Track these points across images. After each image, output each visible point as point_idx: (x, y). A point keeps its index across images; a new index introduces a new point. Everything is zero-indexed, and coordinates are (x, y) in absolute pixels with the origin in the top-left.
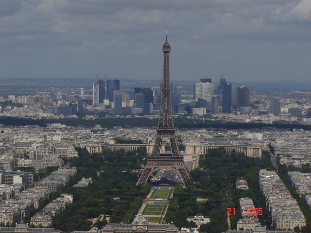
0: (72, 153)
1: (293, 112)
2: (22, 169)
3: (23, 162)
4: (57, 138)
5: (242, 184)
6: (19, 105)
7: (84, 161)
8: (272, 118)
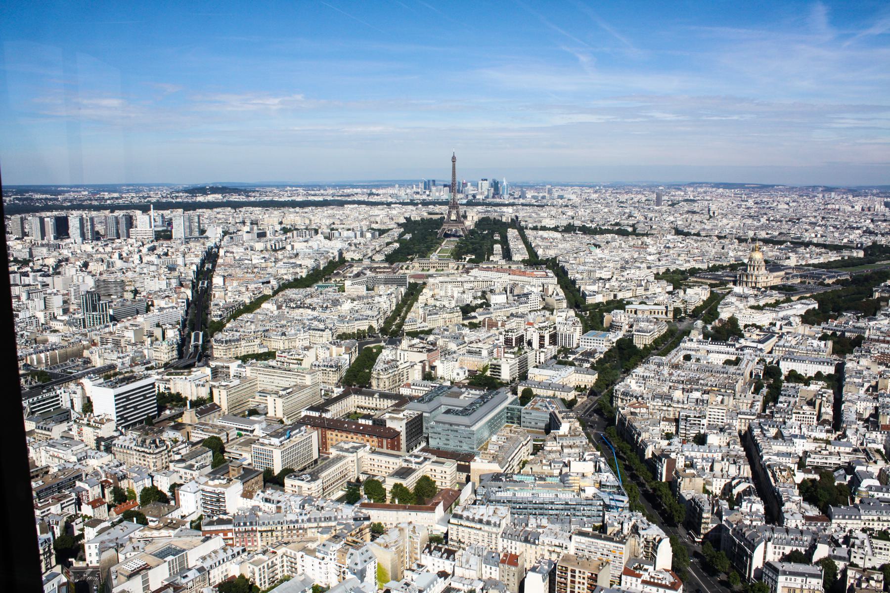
0: (403, 221)
1: (533, 197)
2: (372, 229)
3: (374, 226)
5: (497, 237)
6: (378, 195)
7: (408, 225)
8: (521, 201)
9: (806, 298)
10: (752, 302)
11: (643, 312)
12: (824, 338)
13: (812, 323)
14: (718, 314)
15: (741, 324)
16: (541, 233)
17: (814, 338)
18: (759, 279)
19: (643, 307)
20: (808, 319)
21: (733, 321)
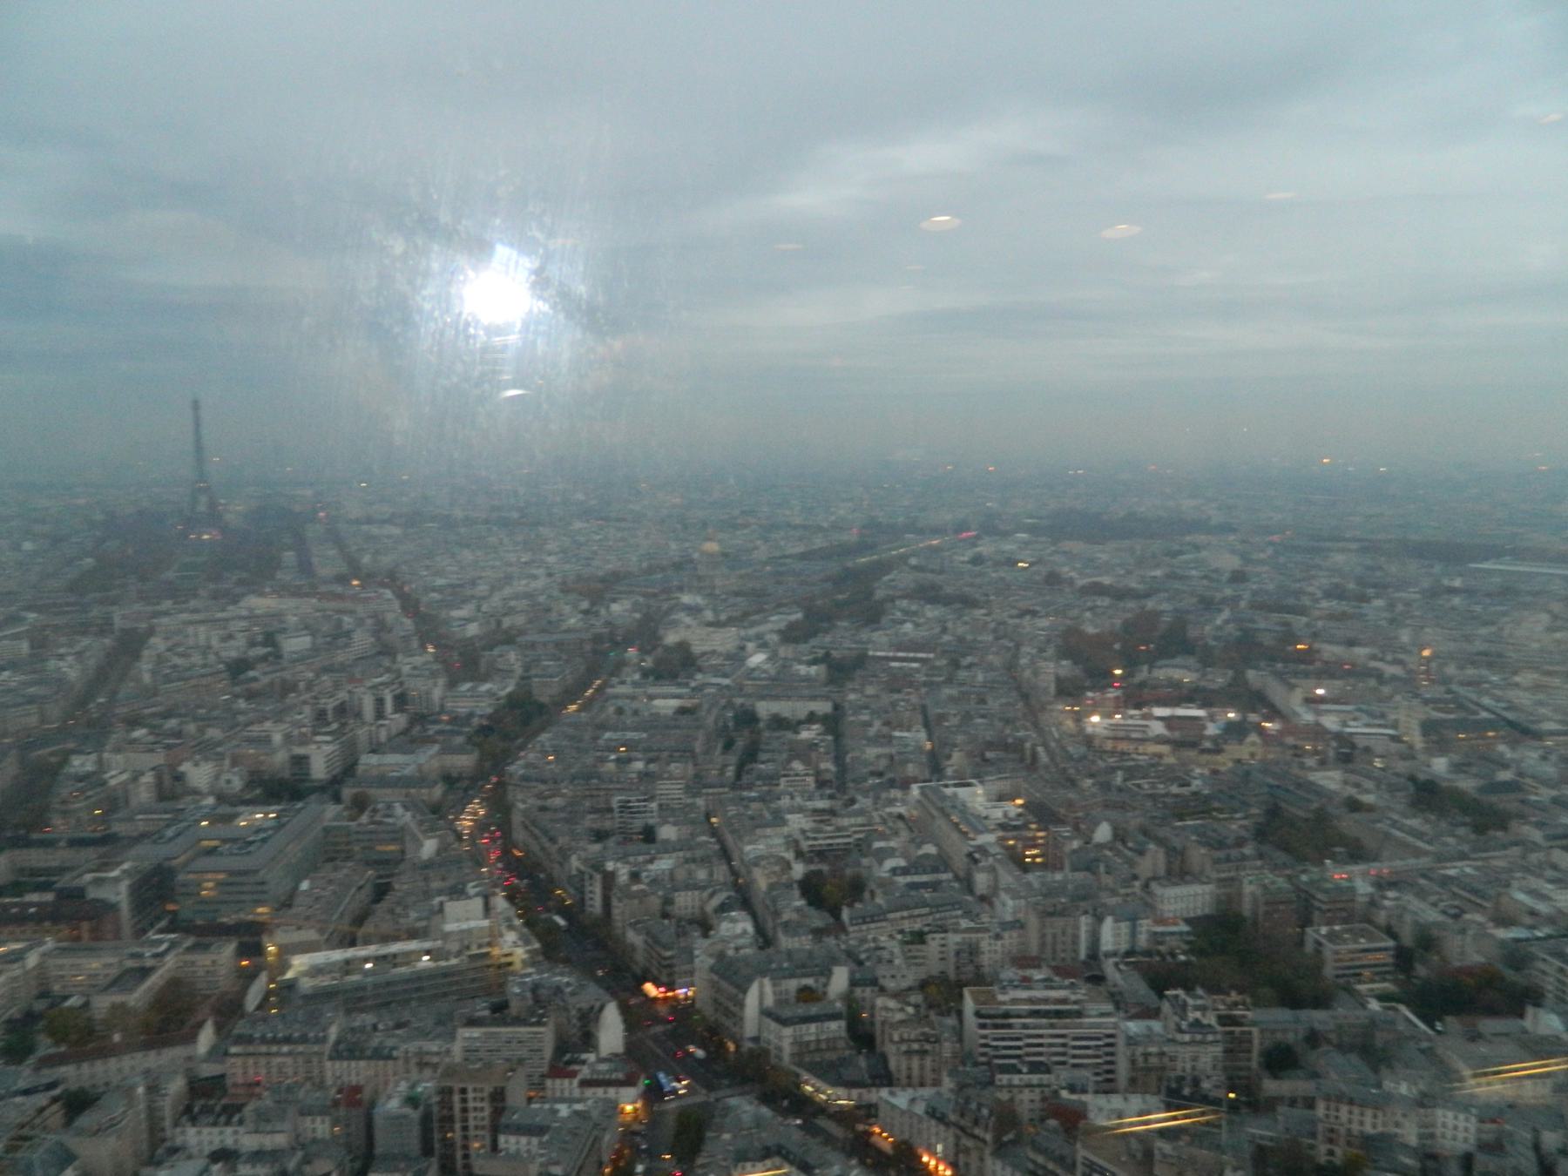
0: (99, 517)
4: (82, 501)
9: (785, 605)
10: (709, 615)
11: (545, 644)
12: (814, 662)
13: (796, 641)
14: (660, 638)
15: (697, 649)
16: (365, 528)
17: (800, 662)
18: (718, 582)
19: (546, 638)
20: (791, 635)
21: (683, 646)
